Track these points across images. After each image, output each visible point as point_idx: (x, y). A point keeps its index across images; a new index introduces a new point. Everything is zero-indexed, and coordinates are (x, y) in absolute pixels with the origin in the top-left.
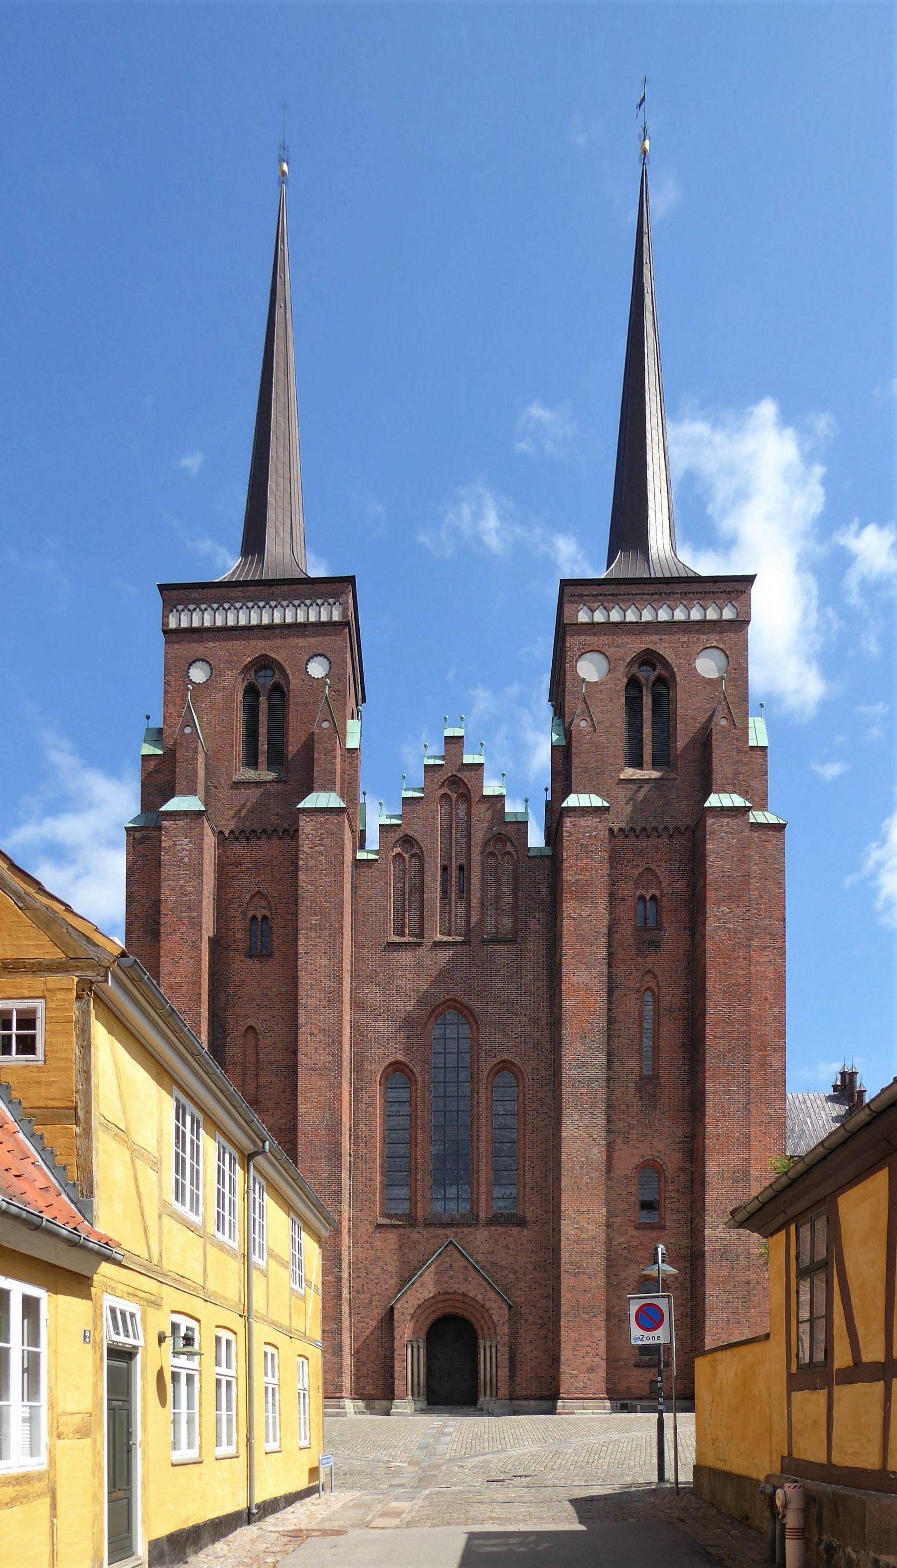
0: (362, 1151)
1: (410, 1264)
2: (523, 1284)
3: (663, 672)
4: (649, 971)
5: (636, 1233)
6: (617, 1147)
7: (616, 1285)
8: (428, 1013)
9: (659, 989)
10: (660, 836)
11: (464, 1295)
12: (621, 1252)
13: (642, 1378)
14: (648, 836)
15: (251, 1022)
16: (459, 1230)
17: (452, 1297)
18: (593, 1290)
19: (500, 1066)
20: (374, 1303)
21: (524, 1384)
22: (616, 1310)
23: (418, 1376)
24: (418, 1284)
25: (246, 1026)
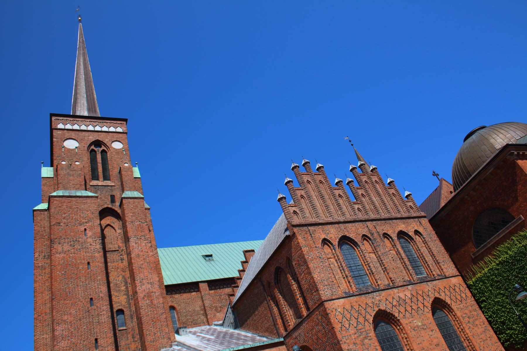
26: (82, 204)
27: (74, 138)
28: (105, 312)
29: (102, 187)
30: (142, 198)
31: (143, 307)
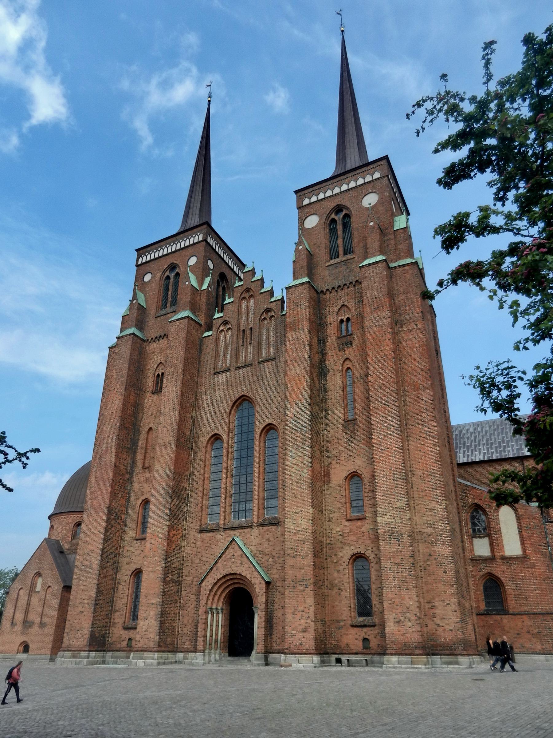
0: (195, 487)
1: (215, 555)
2: (278, 565)
3: (347, 212)
4: (347, 359)
5: (347, 524)
6: (333, 467)
7: (336, 563)
8: (231, 405)
9: (353, 368)
10: (348, 287)
11: (240, 574)
12: (338, 538)
13: (357, 636)
14: (342, 289)
15: (151, 425)
16: (242, 531)
17: (235, 577)
18: (306, 568)
19: (268, 427)
20: (194, 583)
21: (278, 640)
22: (336, 581)
23: (217, 634)
24: (215, 569)
25: (148, 428)
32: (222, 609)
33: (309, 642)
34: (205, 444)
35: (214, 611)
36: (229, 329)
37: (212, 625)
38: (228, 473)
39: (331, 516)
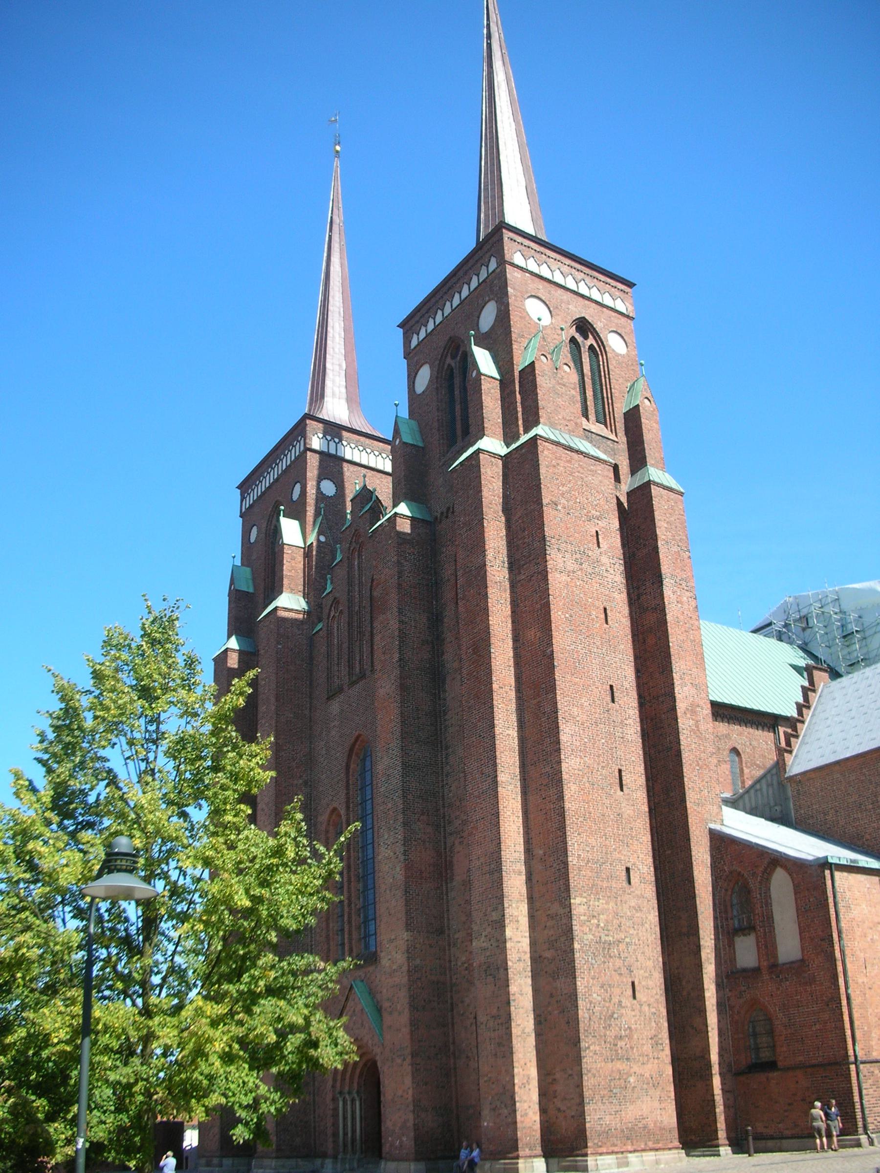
7: (462, 1015)
23: (354, 1131)
26: (589, 473)
27: (543, 298)
28: (630, 721)
29: (598, 437)
30: (682, 493)
31: (684, 731)
32: (358, 1092)
33: (408, 1141)
34: (323, 828)
35: (347, 1096)
36: (341, 612)
37: (345, 1118)
38: (352, 874)
39: (456, 936)
